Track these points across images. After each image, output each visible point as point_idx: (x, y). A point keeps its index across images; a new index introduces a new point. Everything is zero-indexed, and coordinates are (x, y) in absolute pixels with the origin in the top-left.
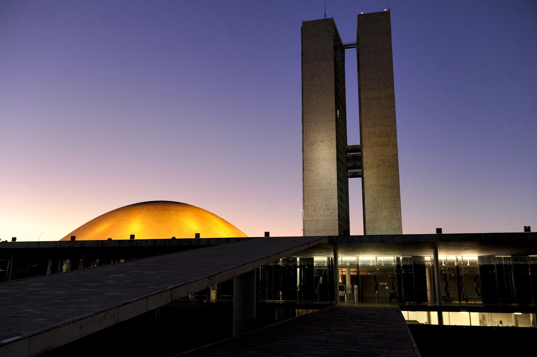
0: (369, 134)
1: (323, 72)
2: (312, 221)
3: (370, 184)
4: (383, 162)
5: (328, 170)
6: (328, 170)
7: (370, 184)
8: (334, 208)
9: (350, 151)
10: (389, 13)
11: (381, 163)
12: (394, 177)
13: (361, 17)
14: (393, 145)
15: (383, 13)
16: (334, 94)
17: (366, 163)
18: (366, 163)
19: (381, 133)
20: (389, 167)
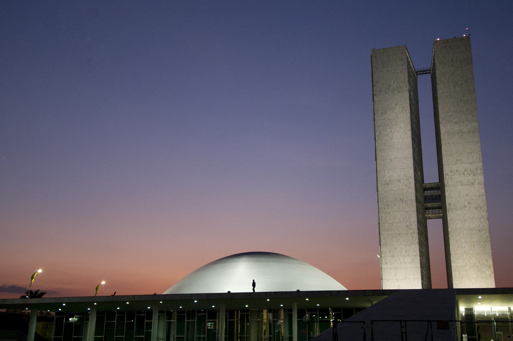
0: (451, 171)
1: (397, 104)
2: (391, 268)
3: (454, 227)
4: (469, 203)
5: (407, 212)
6: (407, 212)
7: (454, 227)
8: (415, 254)
9: (428, 189)
10: (470, 39)
11: (466, 204)
12: (482, 220)
13: (438, 44)
14: (479, 184)
15: (462, 39)
16: (410, 128)
17: (450, 204)
18: (450, 204)
19: (465, 171)
20: (476, 209)
